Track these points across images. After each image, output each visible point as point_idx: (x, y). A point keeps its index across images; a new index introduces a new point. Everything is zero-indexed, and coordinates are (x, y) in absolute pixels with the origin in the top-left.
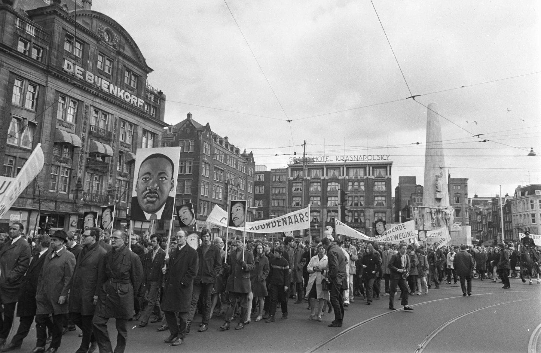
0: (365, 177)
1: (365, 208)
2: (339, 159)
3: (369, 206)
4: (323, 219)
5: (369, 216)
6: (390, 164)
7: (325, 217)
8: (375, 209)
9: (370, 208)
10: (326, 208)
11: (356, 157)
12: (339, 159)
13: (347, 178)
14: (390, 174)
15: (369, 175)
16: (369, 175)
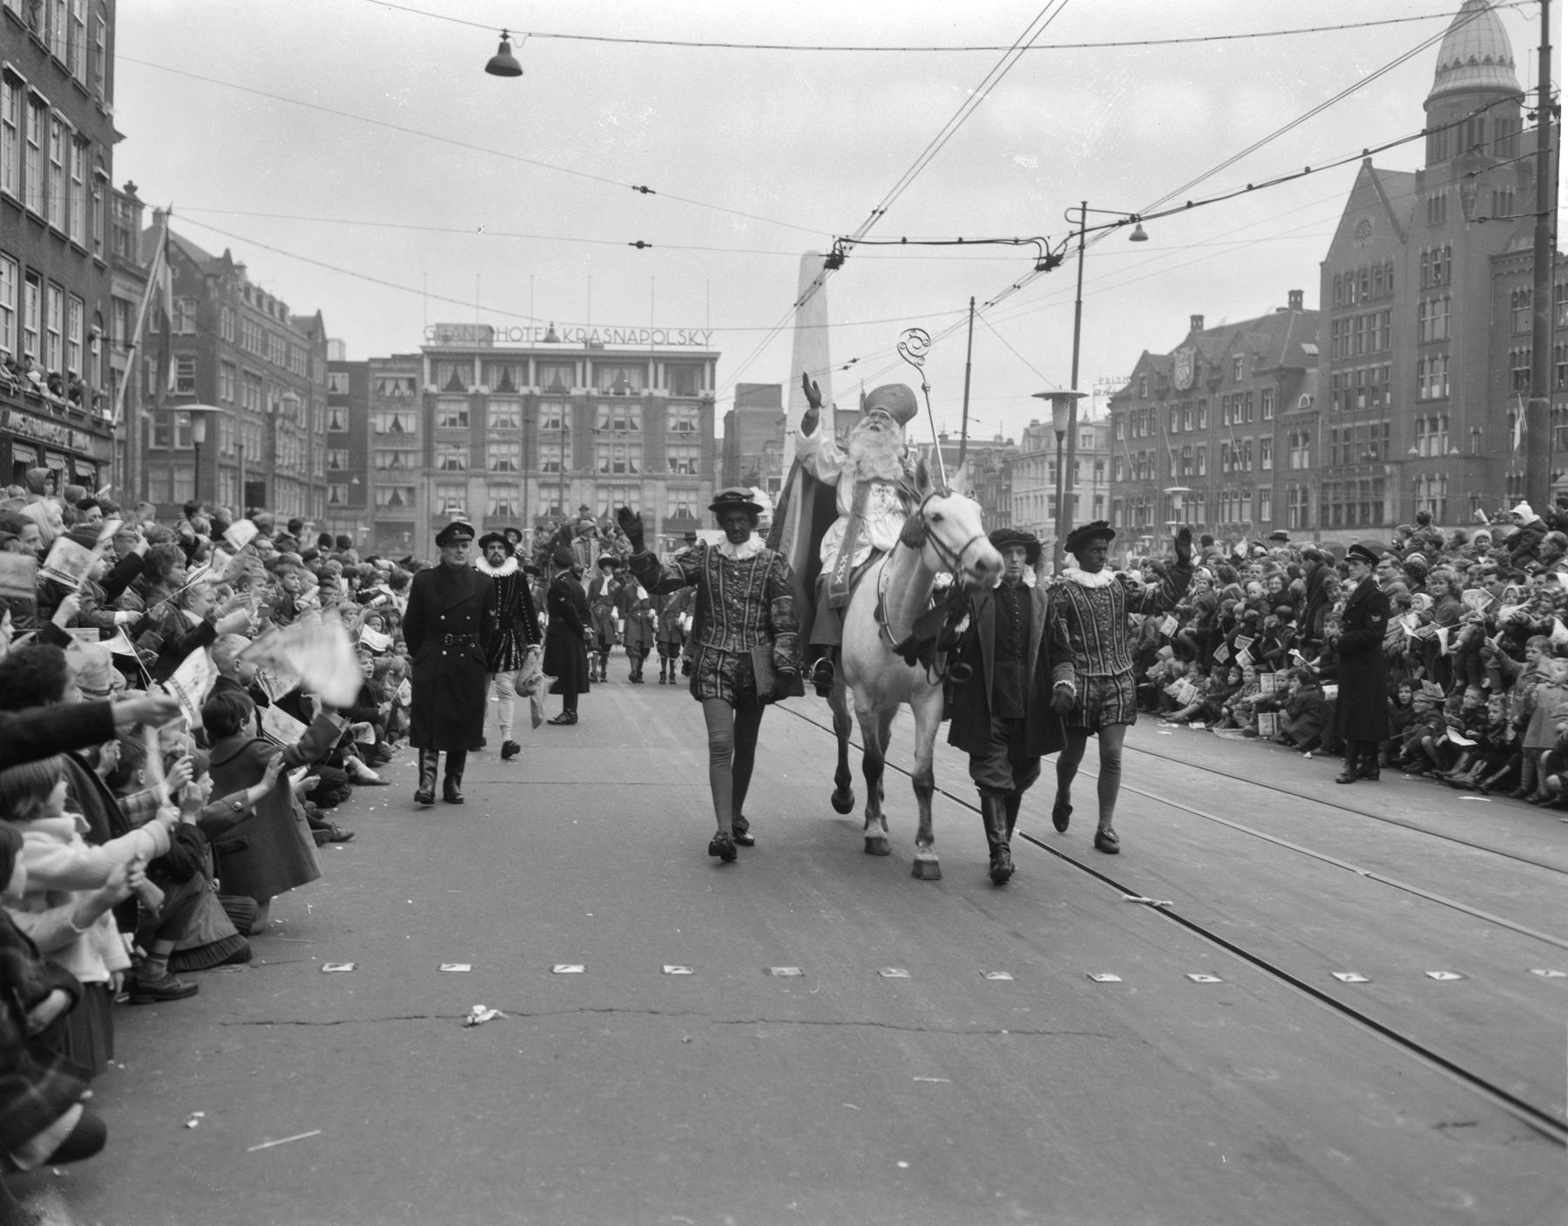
0: (645, 393)
1: (644, 478)
2: (573, 337)
3: (655, 473)
4: (525, 508)
5: (654, 500)
6: (712, 359)
7: (532, 502)
8: (670, 483)
9: (657, 479)
10: (535, 477)
11: (620, 331)
12: (573, 337)
13: (595, 392)
14: (712, 386)
15: (656, 386)
16: (656, 386)
